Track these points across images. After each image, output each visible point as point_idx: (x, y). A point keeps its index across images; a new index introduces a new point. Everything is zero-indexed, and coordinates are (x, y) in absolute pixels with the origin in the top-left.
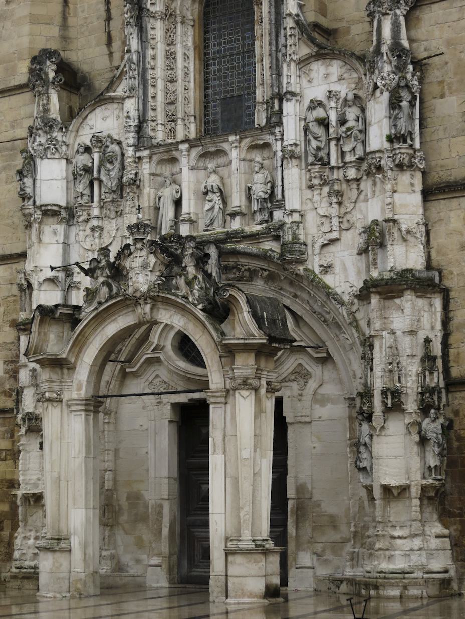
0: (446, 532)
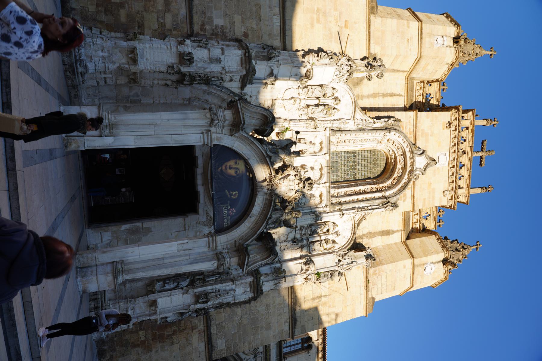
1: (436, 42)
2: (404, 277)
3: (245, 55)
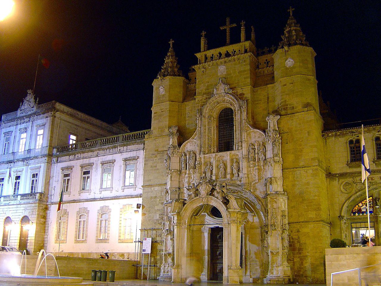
2: (292, 83)
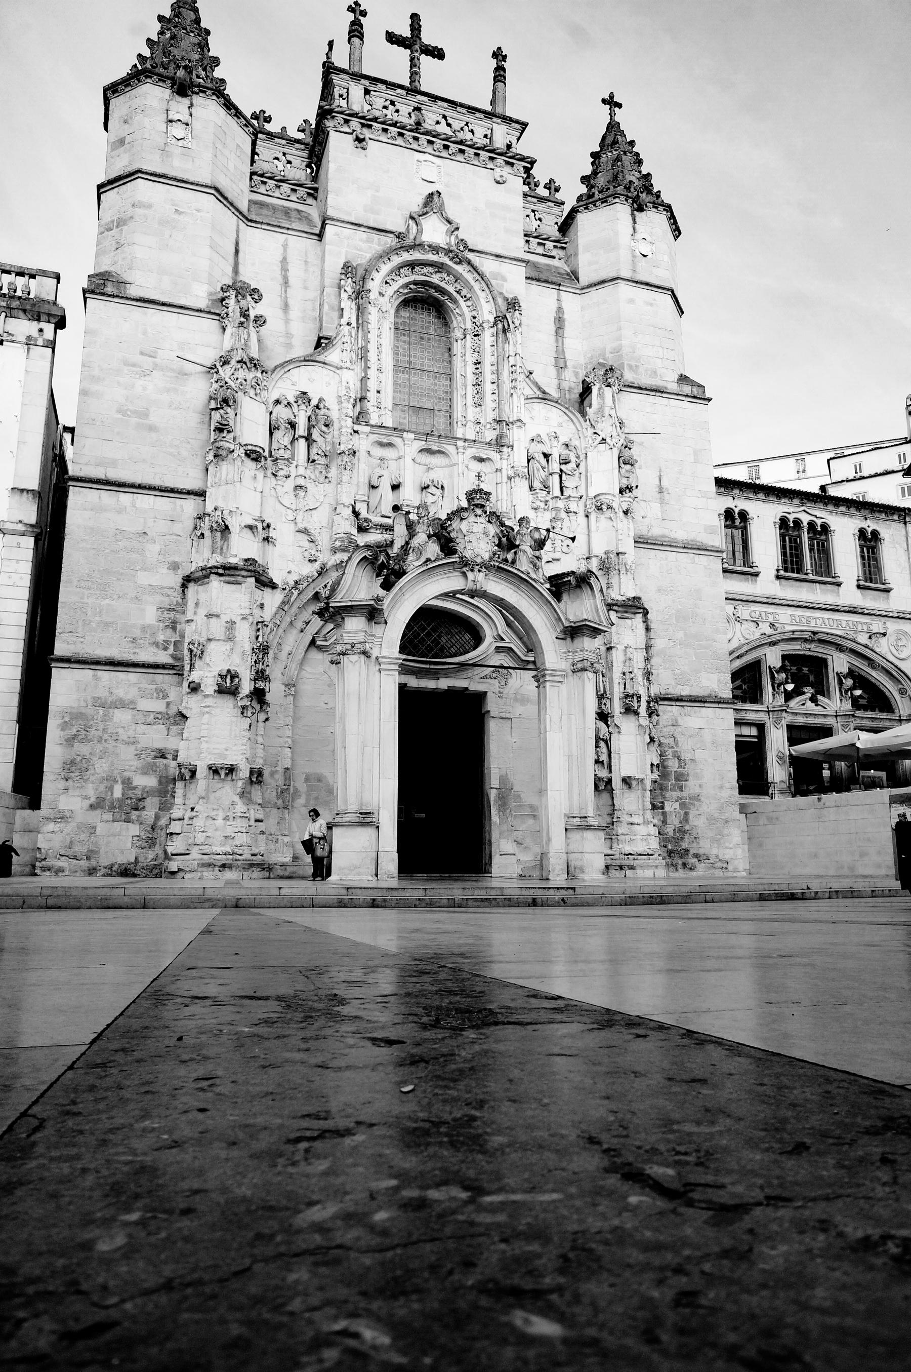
0: (655, 821)
1: (180, 143)
2: (651, 305)
3: (221, 575)
